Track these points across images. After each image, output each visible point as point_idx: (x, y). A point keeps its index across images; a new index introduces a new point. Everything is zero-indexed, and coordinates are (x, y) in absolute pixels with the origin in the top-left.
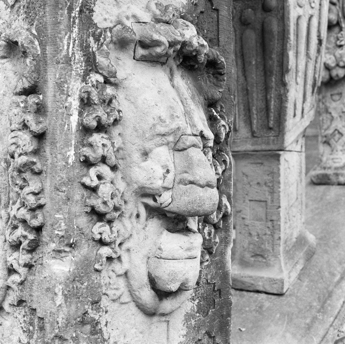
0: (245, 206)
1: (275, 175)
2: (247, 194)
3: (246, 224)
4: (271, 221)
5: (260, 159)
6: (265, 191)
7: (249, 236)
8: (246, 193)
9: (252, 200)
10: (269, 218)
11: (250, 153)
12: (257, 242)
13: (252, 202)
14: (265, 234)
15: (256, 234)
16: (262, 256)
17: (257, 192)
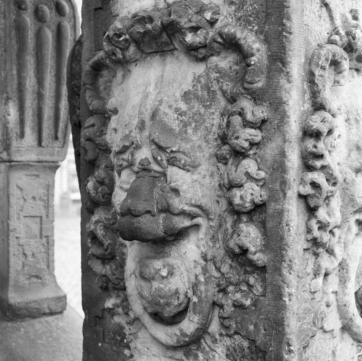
0: (19, 223)
1: (49, 188)
2: (21, 210)
3: (21, 244)
4: (46, 237)
5: (37, 170)
6: (39, 205)
7: (23, 257)
8: (20, 209)
9: (26, 217)
10: (44, 234)
11: (31, 163)
12: (32, 262)
13: (26, 218)
14: (40, 252)
15: (31, 253)
16: (37, 277)
17: (32, 207)
